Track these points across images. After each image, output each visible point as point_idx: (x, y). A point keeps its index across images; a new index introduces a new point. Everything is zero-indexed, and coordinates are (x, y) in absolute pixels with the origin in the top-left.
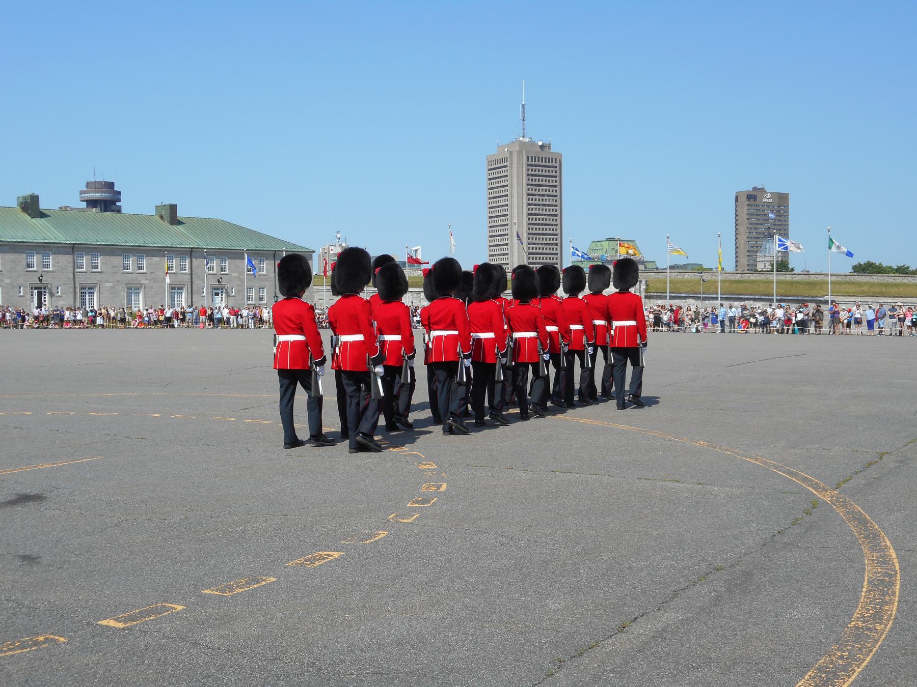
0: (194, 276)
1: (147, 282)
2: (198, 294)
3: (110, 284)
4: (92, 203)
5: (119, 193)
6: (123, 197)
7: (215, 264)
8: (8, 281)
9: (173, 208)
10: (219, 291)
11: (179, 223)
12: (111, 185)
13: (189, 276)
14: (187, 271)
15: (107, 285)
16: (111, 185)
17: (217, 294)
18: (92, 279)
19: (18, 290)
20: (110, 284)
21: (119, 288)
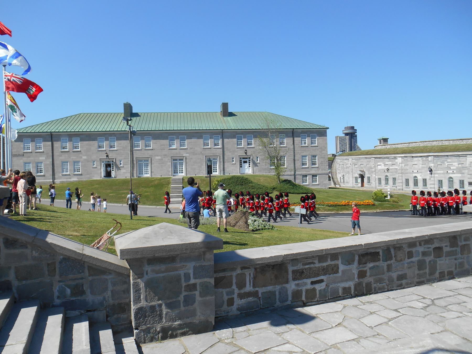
0: (225, 150)
1: (188, 155)
2: (228, 162)
3: (159, 158)
4: (346, 134)
5: (356, 130)
6: (357, 131)
7: (244, 142)
8: (85, 157)
9: (225, 106)
10: (247, 160)
11: (231, 114)
12: (353, 128)
13: (221, 150)
14: (220, 147)
15: (157, 158)
16: (353, 128)
17: (245, 162)
18: (146, 154)
19: (92, 164)
20: (159, 158)
21: (166, 159)
